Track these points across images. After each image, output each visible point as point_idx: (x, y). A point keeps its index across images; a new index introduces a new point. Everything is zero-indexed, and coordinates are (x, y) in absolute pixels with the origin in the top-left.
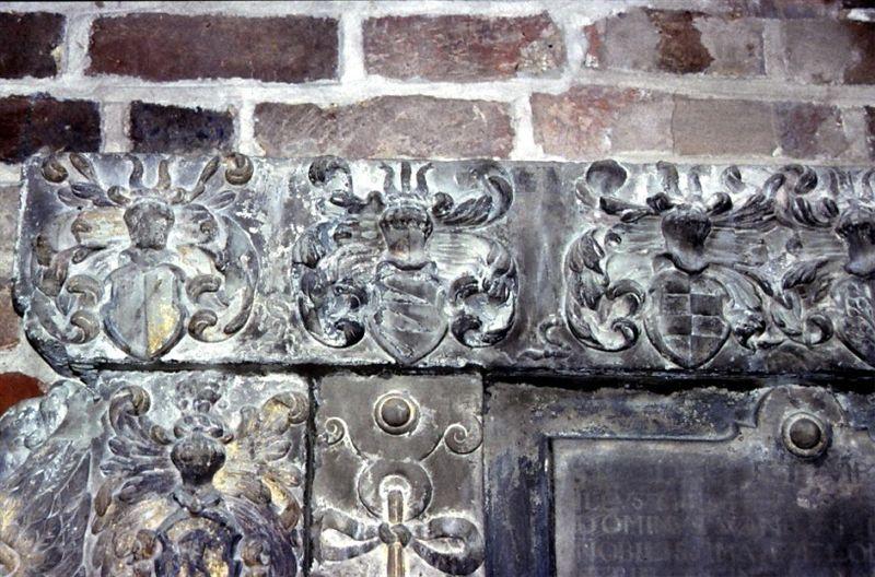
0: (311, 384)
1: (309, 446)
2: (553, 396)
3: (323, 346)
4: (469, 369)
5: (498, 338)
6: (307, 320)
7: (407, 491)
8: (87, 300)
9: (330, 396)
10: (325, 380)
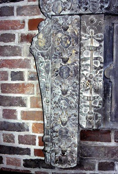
0: (80, 17)
1: (80, 26)
2: (114, 17)
3: (82, 11)
4: (102, 13)
5: (106, 9)
6: (79, 7)
7: (93, 31)
8: (50, 6)
9: (83, 18)
10: (82, 16)
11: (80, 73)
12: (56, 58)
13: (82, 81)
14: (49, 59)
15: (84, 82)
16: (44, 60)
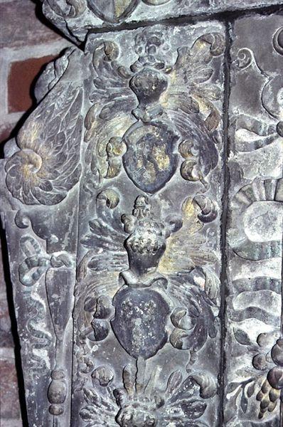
0: (227, 25)
1: (226, 71)
9: (241, 32)
10: (237, 21)
11: (224, 331)
12: (100, 243)
13: (235, 377)
14: (70, 249)
15: (244, 384)
16: (43, 254)
